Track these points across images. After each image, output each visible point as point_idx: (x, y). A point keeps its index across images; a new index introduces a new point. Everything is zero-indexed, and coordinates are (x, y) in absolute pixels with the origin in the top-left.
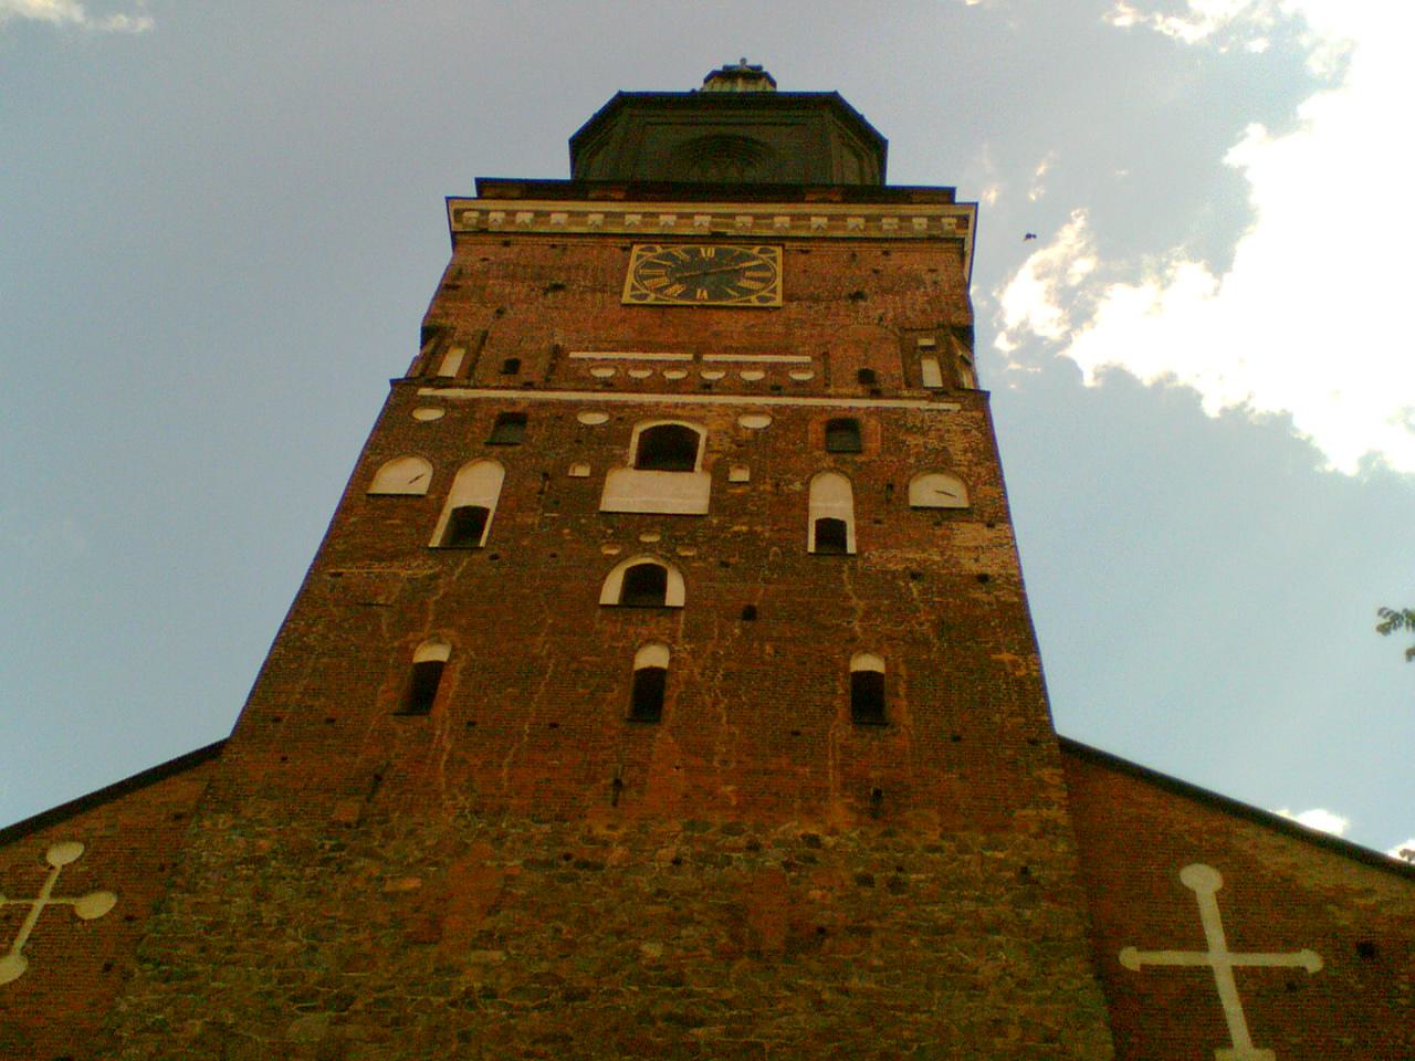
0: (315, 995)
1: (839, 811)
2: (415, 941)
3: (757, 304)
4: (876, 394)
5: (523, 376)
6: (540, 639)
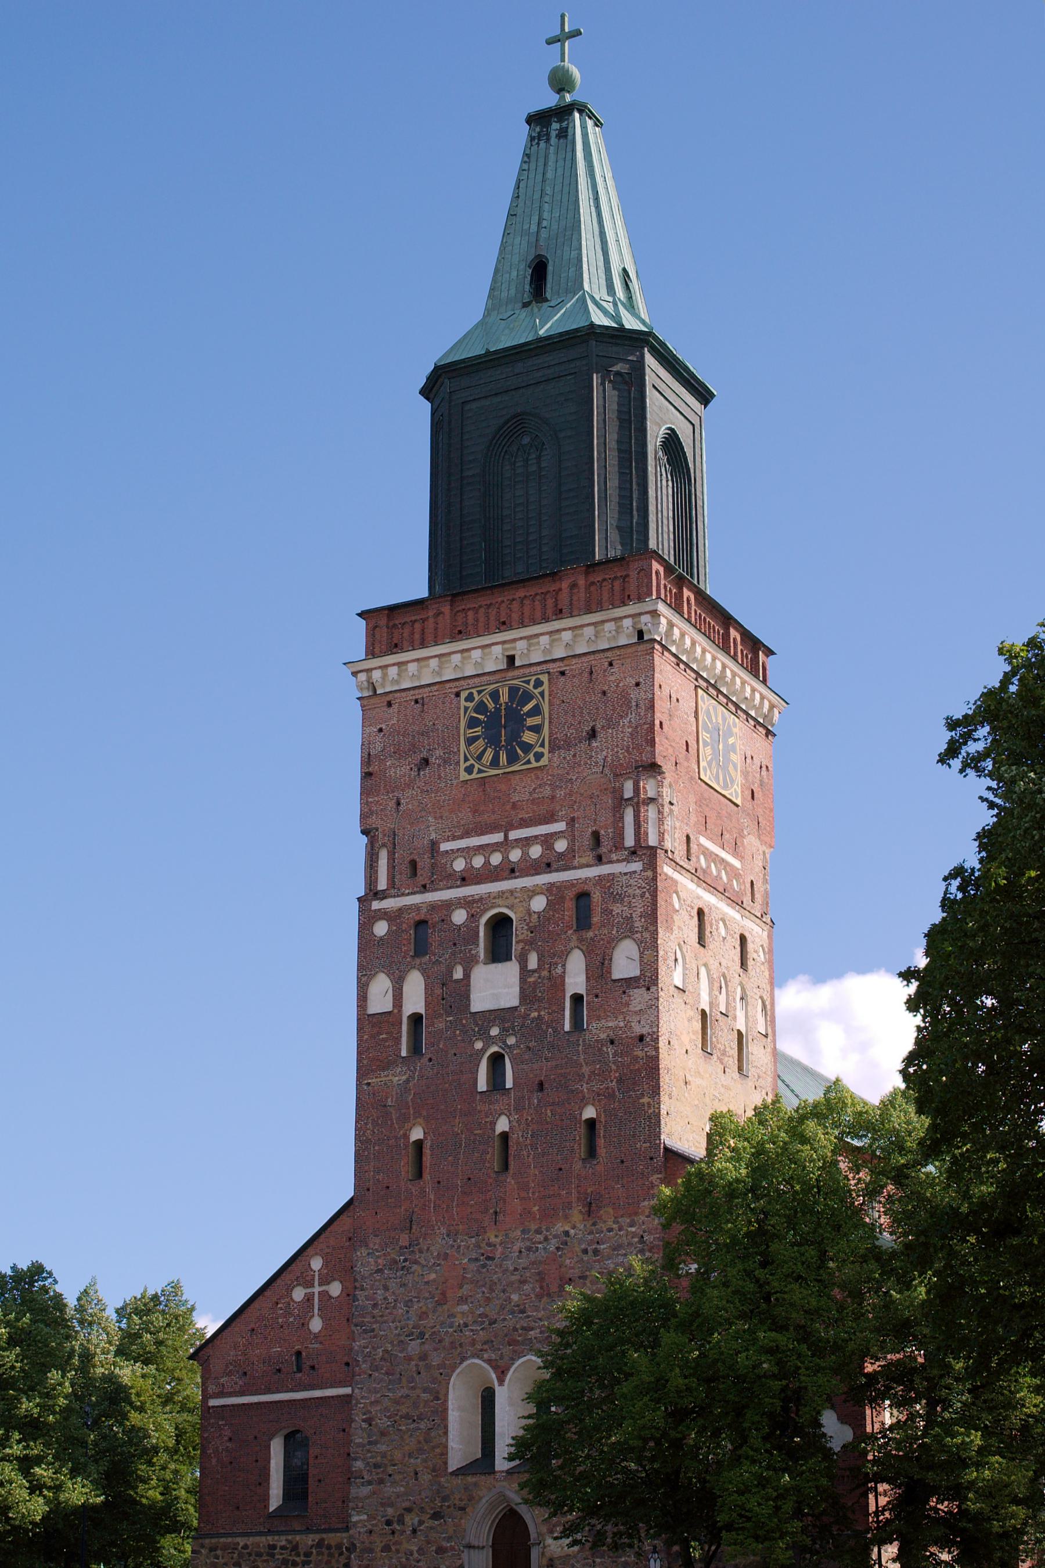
0: (412, 1334)
1: (576, 1215)
2: (439, 1303)
3: (535, 764)
4: (599, 860)
5: (421, 879)
6: (457, 1121)
